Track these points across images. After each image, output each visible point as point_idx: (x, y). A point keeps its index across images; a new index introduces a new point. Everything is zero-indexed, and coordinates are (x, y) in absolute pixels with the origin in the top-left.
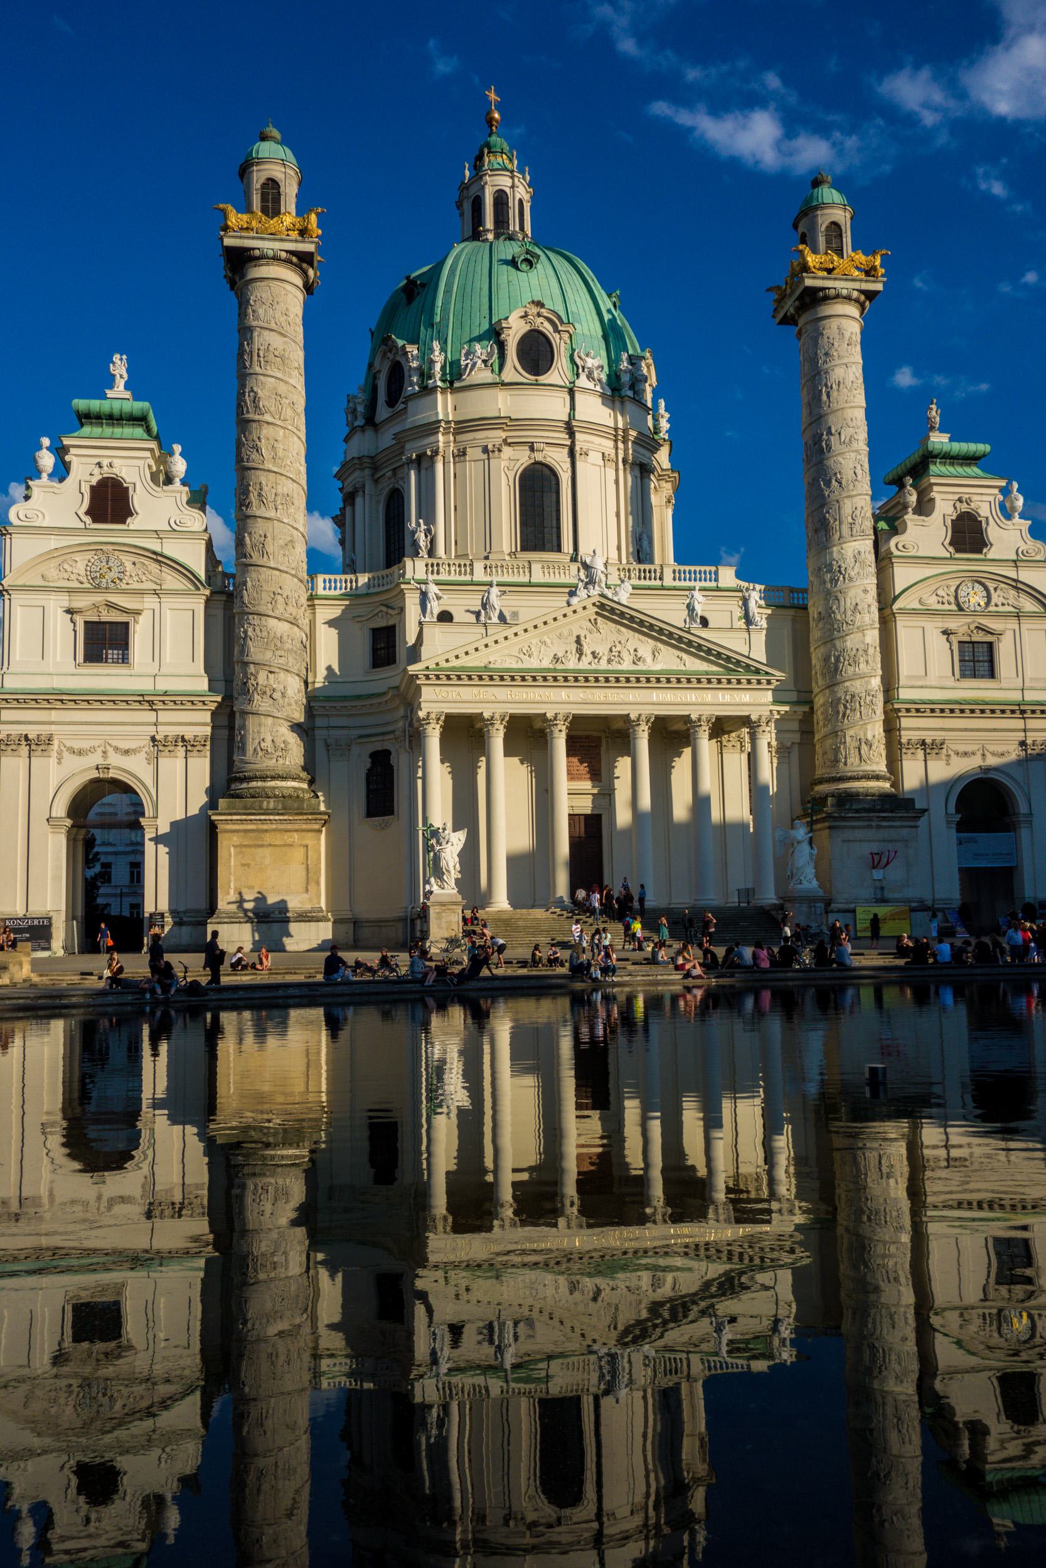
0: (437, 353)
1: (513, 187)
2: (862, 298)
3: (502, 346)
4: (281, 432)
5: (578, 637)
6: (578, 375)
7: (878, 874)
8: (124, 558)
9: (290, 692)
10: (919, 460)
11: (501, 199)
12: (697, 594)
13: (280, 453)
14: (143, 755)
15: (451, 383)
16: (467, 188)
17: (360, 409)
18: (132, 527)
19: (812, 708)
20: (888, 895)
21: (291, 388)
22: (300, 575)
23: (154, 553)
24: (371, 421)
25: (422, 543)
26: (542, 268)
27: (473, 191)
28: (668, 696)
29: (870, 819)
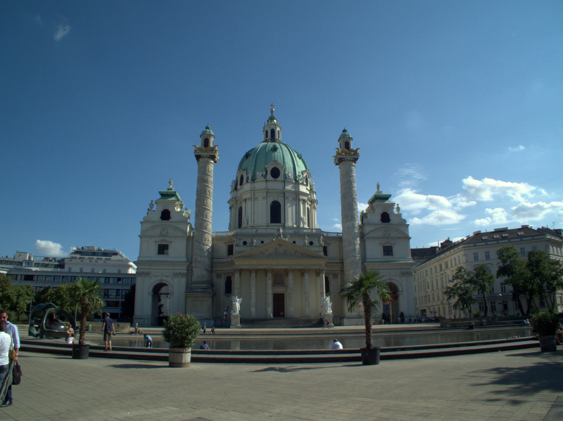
0: (250, 173)
1: (276, 128)
2: (354, 160)
3: (267, 171)
5: (275, 249)
10: (374, 198)
11: (273, 132)
12: (306, 237)
13: (205, 203)
15: (254, 180)
17: (233, 186)
19: (343, 265)
20: (360, 314)
22: (209, 233)
23: (176, 227)
24: (236, 189)
25: (245, 221)
26: (279, 150)
27: (266, 129)
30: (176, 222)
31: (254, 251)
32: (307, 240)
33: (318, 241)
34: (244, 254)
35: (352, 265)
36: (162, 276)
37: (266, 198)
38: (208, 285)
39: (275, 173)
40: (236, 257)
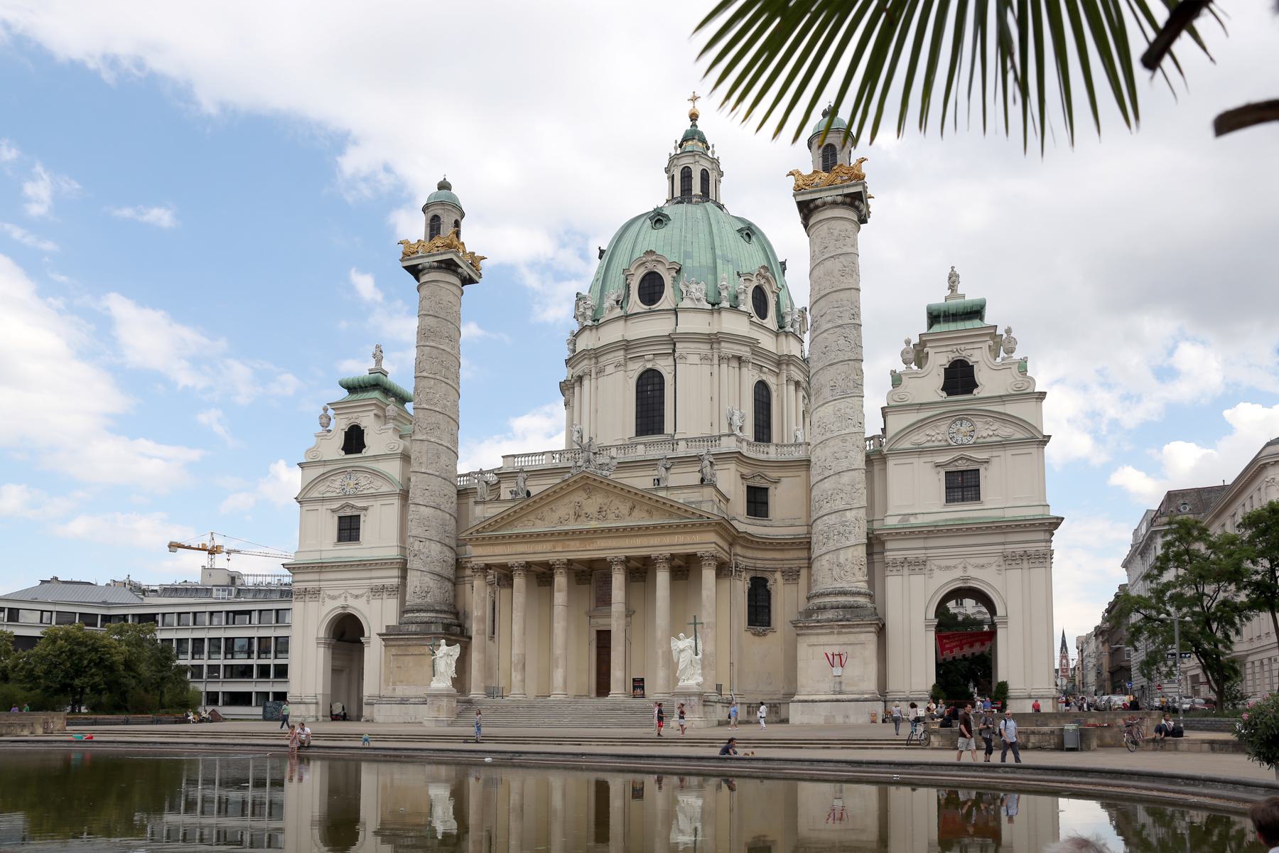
3: (628, 287)
4: (432, 381)
6: (682, 299)
7: (837, 671)
8: (359, 475)
9: (433, 554)
11: (686, 175)
14: (365, 598)
15: (598, 320)
16: (669, 170)
18: (366, 455)
20: (844, 688)
21: (441, 352)
22: (443, 475)
23: (373, 470)
28: (638, 541)
29: (831, 627)
30: (376, 458)
31: (515, 512)
32: (667, 469)
33: (699, 469)
34: (490, 524)
35: (828, 538)
36: (346, 597)
37: (625, 365)
38: (440, 615)
39: (651, 288)
40: (471, 534)
